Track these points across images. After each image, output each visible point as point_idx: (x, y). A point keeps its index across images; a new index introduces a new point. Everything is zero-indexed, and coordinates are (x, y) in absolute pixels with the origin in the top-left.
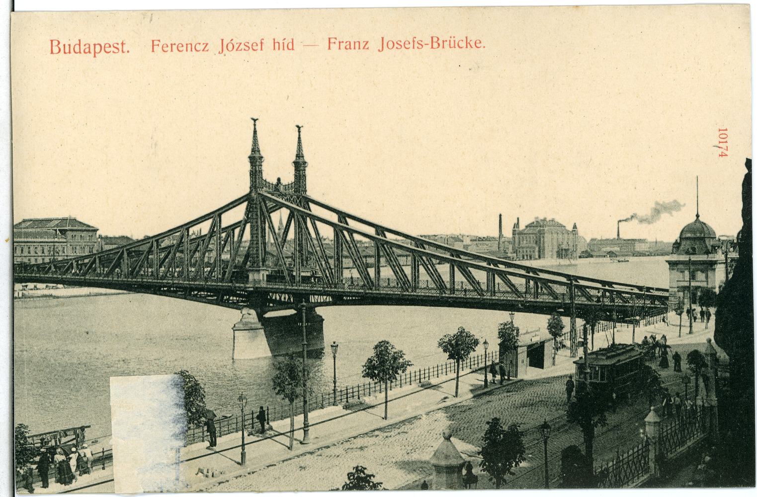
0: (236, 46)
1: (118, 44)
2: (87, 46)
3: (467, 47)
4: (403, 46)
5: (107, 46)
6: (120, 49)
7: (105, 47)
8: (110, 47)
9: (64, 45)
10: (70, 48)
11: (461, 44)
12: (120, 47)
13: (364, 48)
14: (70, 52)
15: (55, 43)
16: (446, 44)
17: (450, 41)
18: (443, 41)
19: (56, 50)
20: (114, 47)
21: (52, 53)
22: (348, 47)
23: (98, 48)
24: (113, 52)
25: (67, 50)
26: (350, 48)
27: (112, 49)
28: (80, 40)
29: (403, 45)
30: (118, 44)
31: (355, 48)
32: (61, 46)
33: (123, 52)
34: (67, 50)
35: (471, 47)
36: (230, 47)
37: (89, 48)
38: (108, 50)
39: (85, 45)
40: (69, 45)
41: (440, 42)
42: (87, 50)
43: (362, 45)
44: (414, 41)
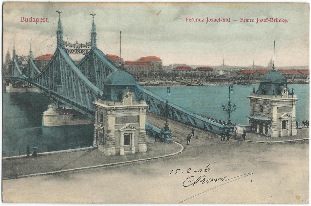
0: (211, 20)
3: (282, 22)
6: (46, 20)
9: (26, 19)
10: (28, 20)
11: (280, 21)
15: (22, 18)
16: (275, 20)
17: (276, 20)
18: (274, 20)
19: (23, 20)
23: (38, 20)
24: (44, 21)
33: (47, 22)
35: (283, 22)
36: (210, 20)
38: (41, 20)
40: (27, 19)
41: (273, 20)
42: (34, 21)
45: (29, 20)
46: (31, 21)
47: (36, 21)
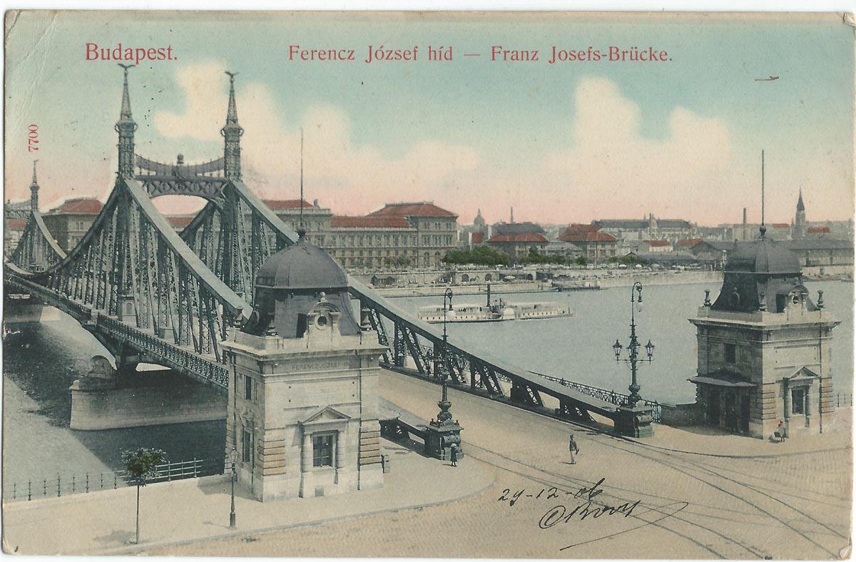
1: (164, 49)
2: (129, 51)
4: (403, 58)
6: (167, 55)
7: (148, 53)
8: (155, 52)
9: (102, 50)
12: (166, 52)
14: (109, 58)
15: (92, 47)
21: (88, 58)
22: (514, 58)
23: (141, 54)
24: (159, 58)
25: (106, 56)
28: (120, 45)
29: (402, 56)
30: (164, 49)
32: (99, 51)
33: (169, 58)
34: (106, 56)
37: (131, 54)
39: (126, 51)
40: (108, 50)
42: (128, 56)
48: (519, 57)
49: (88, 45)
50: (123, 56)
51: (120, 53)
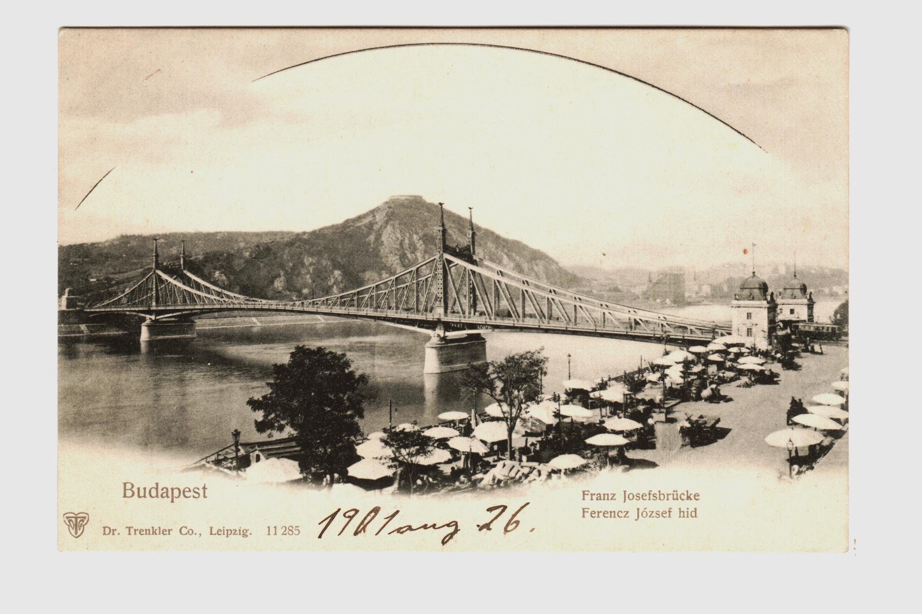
2: (165, 490)
5: (187, 490)
7: (184, 492)
9: (139, 489)
10: (145, 491)
12: (201, 492)
13: (612, 499)
14: (145, 496)
15: (128, 486)
19: (129, 493)
20: (194, 492)
21: (125, 496)
22: (599, 498)
23: (176, 492)
24: (194, 497)
25: (142, 494)
26: (600, 499)
27: (192, 493)
31: (604, 499)
34: (142, 494)
37: (167, 492)
38: (187, 494)
39: (162, 489)
42: (164, 495)
43: (610, 497)
44: (650, 494)
45: (150, 491)
46: (157, 496)
47: (170, 494)
48: (602, 498)
49: (125, 484)
50: (159, 495)
51: (157, 492)
